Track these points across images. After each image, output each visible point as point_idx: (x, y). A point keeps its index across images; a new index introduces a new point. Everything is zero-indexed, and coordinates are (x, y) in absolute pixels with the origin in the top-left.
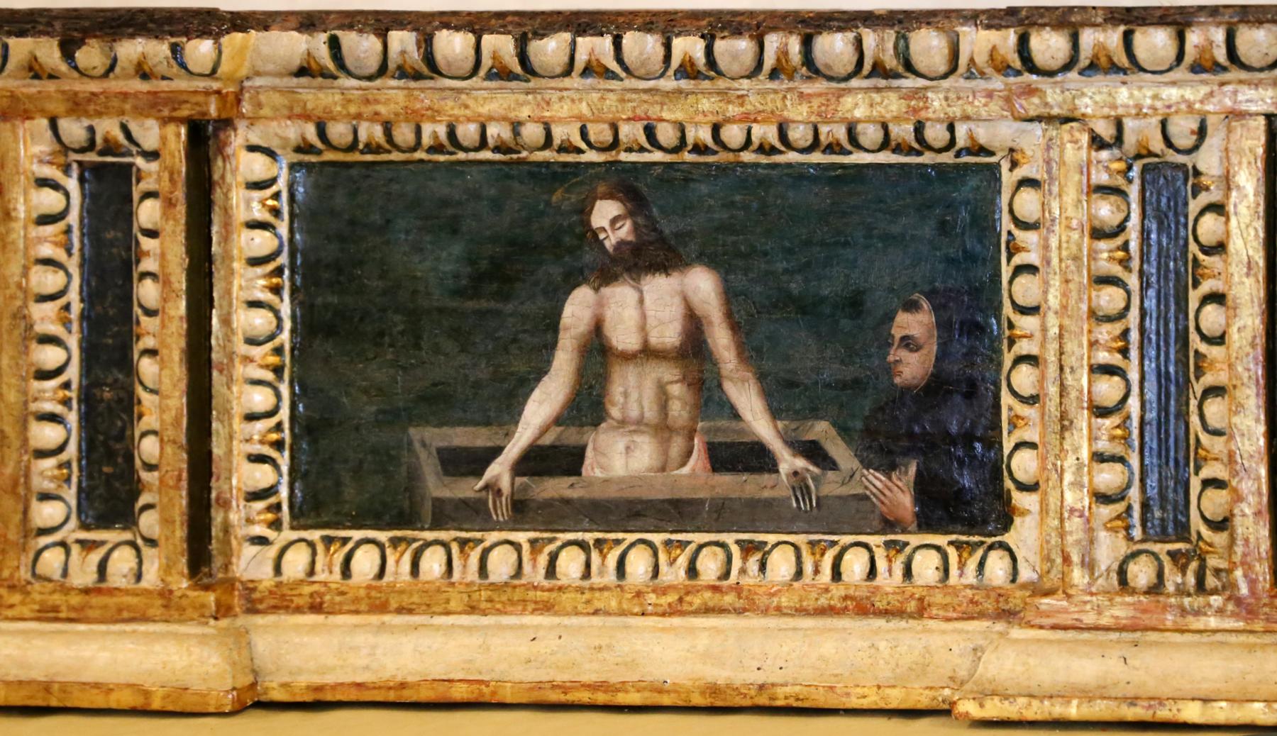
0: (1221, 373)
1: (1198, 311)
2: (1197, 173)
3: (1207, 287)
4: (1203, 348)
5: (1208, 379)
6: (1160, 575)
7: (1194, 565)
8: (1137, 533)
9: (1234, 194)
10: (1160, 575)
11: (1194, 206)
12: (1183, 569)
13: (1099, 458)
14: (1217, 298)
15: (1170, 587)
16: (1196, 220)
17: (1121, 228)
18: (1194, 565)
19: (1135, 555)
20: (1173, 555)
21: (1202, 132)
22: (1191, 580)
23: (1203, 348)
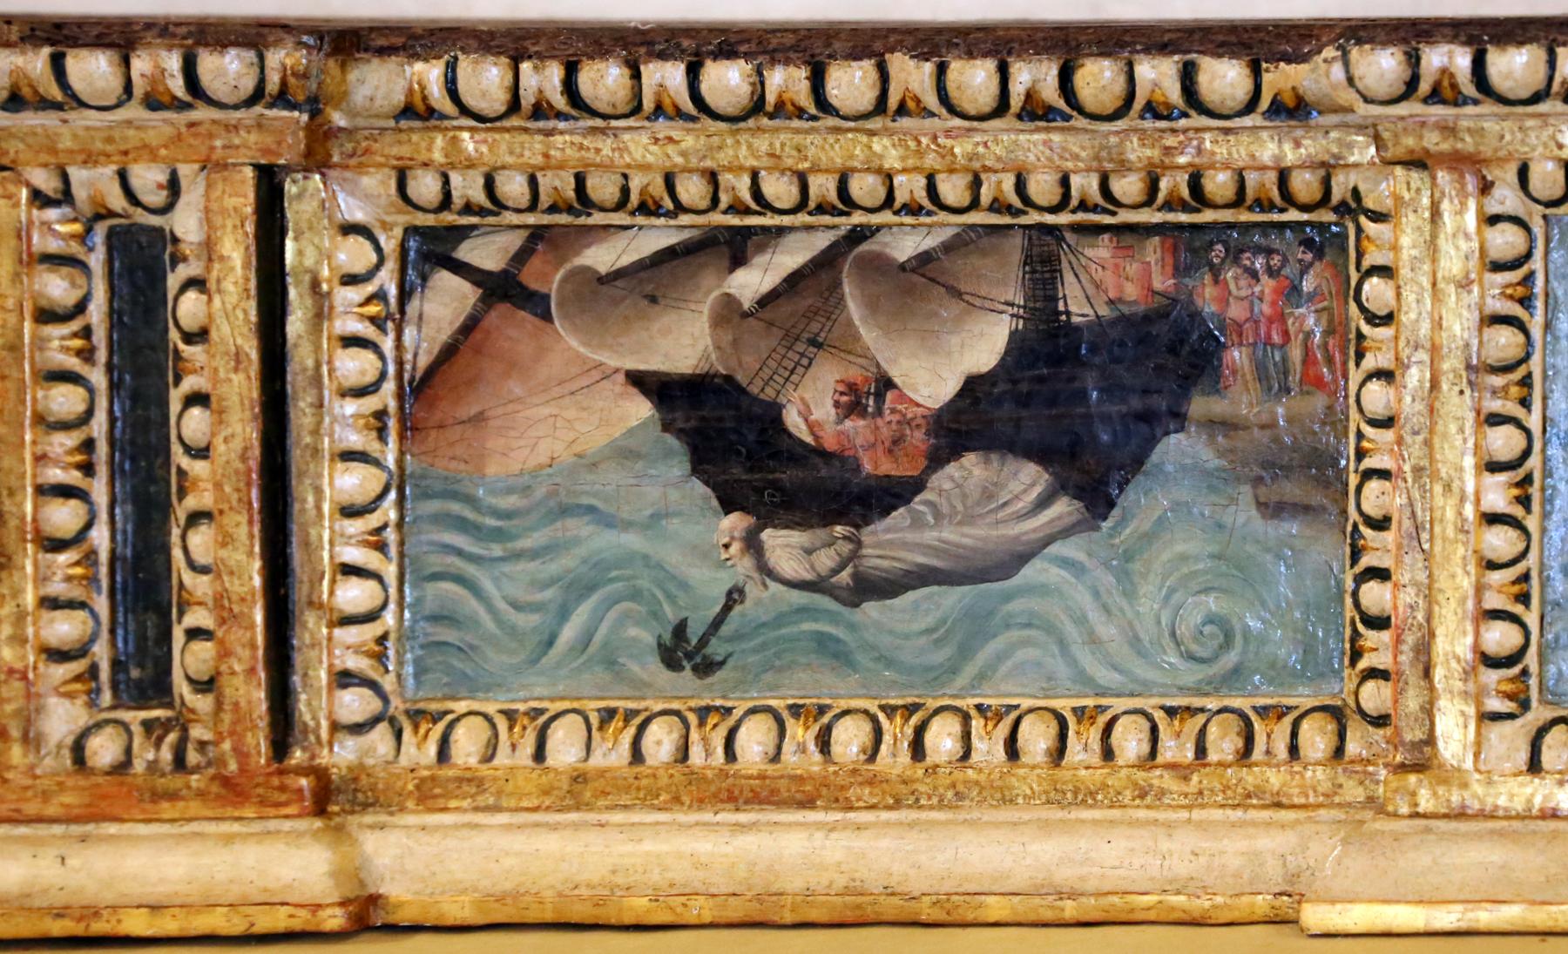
0: (206, 493)
1: (180, 416)
2: (176, 240)
3: (189, 384)
4: (185, 462)
5: (191, 502)
6: (128, 751)
7: (172, 737)
8: (107, 698)
9: (217, 266)
10: (128, 751)
11: (173, 281)
12: (158, 745)
13: (51, 603)
14: (198, 399)
15: (139, 766)
16: (176, 299)
17: (81, 307)
18: (172, 737)
19: (99, 726)
20: (148, 725)
21: (173, 186)
22: (166, 755)
23: (185, 462)
